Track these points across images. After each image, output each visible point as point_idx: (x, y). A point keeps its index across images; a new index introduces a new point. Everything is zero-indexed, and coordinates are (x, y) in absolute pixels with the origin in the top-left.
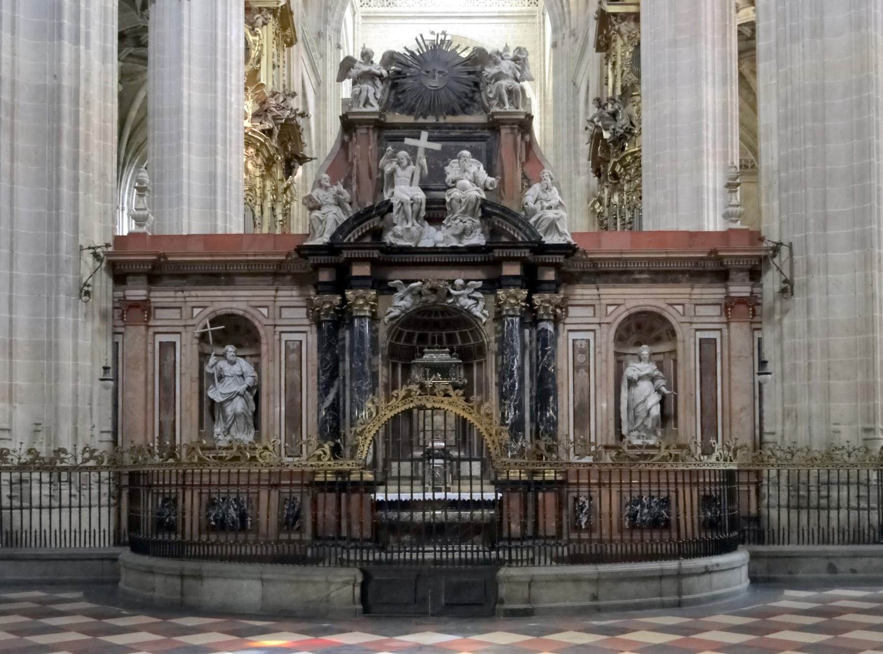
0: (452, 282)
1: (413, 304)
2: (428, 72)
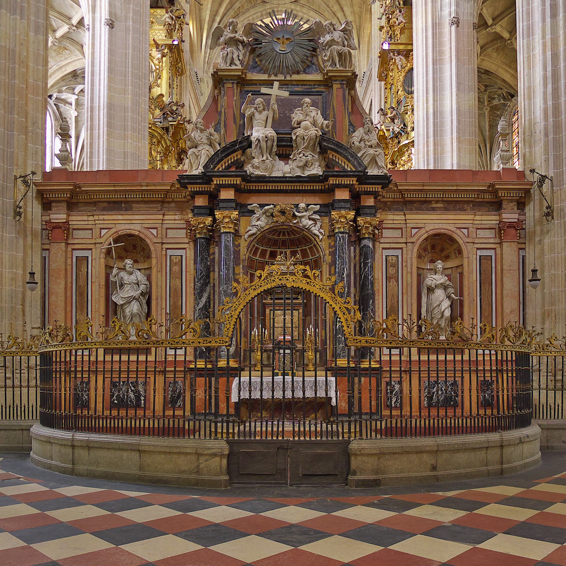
2: (278, 39)
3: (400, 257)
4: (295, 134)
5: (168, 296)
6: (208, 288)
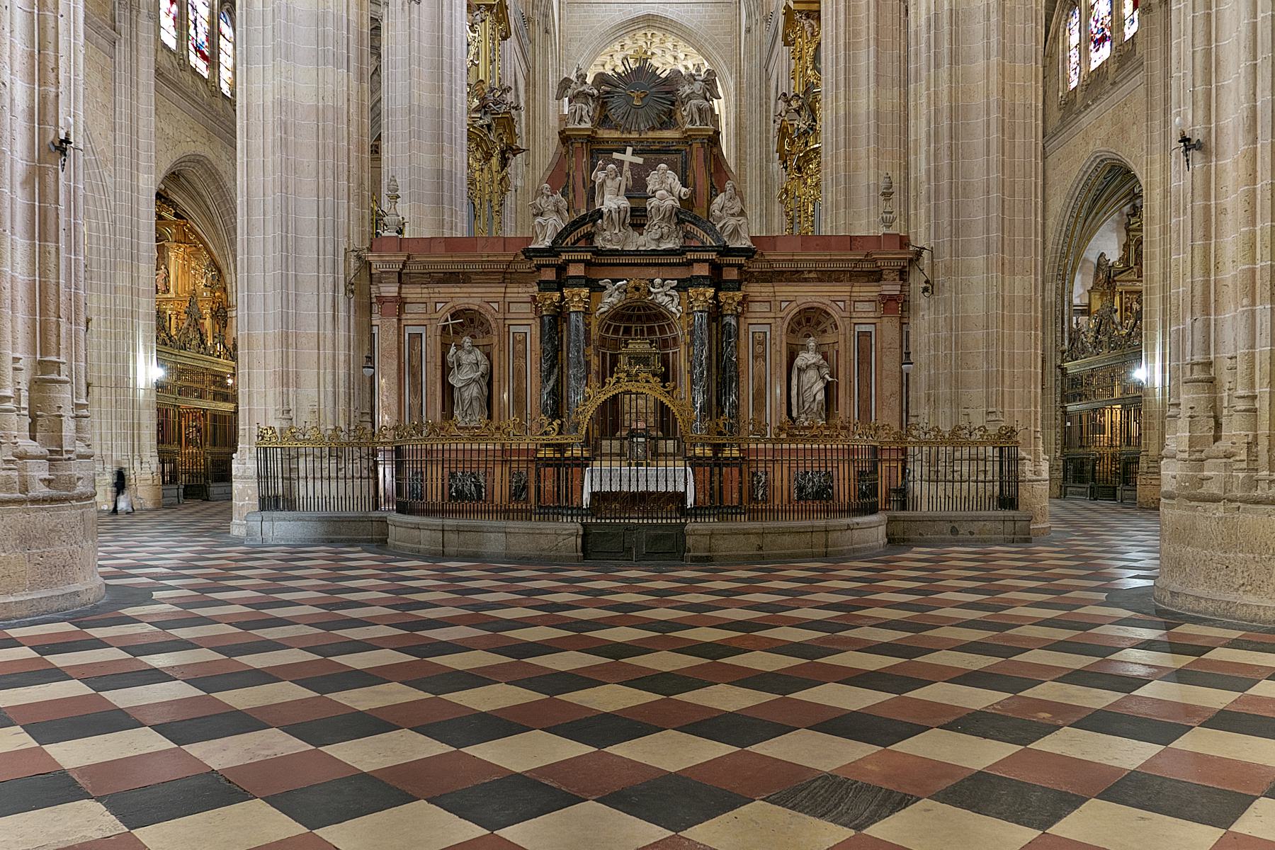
0: (652, 281)
1: (620, 301)
3: (768, 333)
4: (650, 204)
5: (511, 378)
6: (556, 370)
